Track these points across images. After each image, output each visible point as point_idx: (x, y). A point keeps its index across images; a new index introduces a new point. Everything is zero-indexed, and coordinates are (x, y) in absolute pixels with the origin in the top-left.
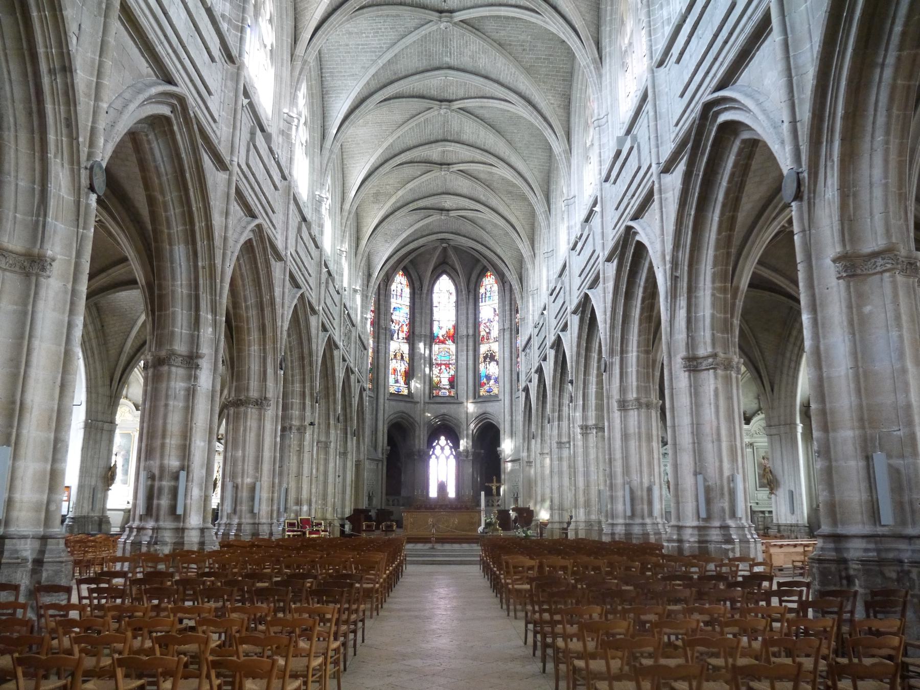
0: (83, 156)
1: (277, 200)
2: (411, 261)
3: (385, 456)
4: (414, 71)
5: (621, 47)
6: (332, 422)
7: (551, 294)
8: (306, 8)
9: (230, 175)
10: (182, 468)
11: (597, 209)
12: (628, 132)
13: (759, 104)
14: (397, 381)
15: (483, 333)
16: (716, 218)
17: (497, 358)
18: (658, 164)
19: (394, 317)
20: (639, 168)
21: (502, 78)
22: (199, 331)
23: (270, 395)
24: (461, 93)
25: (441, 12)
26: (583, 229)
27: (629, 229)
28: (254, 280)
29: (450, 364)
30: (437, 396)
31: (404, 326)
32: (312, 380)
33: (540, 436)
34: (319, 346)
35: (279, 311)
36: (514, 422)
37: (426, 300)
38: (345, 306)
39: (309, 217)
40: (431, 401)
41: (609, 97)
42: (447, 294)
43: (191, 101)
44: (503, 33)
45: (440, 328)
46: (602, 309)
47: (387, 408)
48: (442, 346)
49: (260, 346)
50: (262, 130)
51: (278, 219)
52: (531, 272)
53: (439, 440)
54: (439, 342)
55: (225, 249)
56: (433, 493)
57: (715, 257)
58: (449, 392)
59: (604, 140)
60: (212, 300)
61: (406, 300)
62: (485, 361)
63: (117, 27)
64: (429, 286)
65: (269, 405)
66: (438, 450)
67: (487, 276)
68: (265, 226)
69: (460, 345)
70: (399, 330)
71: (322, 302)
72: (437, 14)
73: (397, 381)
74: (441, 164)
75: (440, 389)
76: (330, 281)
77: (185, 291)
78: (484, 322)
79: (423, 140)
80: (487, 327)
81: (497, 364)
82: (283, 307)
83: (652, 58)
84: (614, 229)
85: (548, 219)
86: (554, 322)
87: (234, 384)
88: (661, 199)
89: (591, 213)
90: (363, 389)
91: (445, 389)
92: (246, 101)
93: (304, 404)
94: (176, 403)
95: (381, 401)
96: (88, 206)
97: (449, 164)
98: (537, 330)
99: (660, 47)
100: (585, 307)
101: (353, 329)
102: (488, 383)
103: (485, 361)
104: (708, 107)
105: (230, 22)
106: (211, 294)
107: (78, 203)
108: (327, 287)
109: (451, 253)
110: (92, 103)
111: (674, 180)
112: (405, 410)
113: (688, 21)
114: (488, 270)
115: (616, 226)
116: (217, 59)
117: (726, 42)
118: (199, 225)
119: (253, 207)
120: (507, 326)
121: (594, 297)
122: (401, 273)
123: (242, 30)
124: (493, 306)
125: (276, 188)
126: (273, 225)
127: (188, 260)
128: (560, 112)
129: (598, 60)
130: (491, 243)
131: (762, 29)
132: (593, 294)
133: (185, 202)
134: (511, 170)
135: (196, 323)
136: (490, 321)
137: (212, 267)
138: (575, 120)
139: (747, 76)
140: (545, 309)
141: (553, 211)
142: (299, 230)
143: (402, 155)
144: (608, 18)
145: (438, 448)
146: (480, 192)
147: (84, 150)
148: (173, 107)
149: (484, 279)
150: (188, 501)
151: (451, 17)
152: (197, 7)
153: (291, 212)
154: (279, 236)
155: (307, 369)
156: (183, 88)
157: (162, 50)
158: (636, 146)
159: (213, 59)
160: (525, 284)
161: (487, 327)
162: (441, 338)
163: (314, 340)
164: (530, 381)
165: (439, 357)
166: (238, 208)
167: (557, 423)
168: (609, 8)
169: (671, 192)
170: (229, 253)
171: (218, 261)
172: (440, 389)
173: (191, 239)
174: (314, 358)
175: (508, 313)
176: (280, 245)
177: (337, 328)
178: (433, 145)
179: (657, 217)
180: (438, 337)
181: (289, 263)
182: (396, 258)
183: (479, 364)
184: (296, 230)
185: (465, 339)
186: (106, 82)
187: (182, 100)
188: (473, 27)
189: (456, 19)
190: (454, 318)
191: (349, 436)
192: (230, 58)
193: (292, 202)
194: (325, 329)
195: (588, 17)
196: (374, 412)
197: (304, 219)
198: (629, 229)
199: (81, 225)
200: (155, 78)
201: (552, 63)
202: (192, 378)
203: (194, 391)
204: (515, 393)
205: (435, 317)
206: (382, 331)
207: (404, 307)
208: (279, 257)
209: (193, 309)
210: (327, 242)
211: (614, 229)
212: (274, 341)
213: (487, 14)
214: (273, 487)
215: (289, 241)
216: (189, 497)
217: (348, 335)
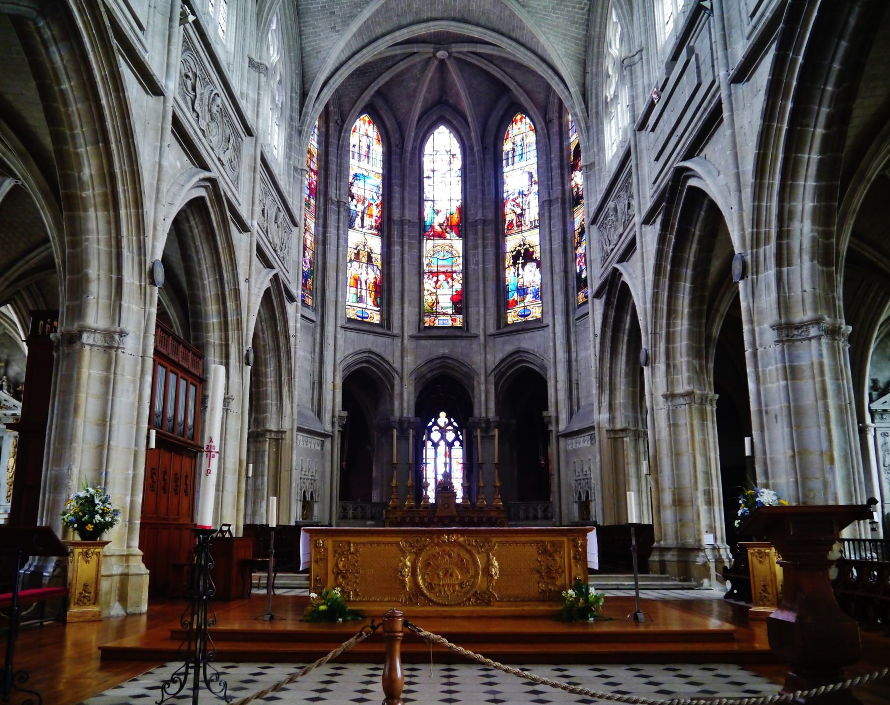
3: (337, 428)
14: (360, 299)
15: (510, 217)
17: (537, 255)
19: (354, 190)
29: (453, 272)
31: (374, 207)
33: (662, 358)
36: (574, 364)
37: (412, 162)
40: (423, 334)
42: (447, 157)
47: (340, 342)
53: (437, 417)
54: (433, 236)
58: (454, 320)
61: (377, 165)
62: (515, 264)
64: (415, 140)
66: (436, 436)
67: (516, 121)
69: (471, 237)
70: (363, 213)
73: (360, 299)
75: (437, 314)
78: (511, 197)
80: (518, 205)
91: (444, 314)
95: (330, 328)
101: (247, 140)
102: (523, 300)
109: (455, 75)
112: (374, 349)
120: (557, 192)
124: (527, 169)
136: (522, 194)
149: (510, 128)
161: (518, 205)
162: (438, 228)
165: (434, 260)
167: (772, 272)
172: (437, 314)
175: (556, 172)
180: (432, 227)
183: (505, 269)
190: (459, 196)
196: (317, 349)
204: (575, 310)
205: (428, 193)
206: (333, 207)
207: (372, 175)
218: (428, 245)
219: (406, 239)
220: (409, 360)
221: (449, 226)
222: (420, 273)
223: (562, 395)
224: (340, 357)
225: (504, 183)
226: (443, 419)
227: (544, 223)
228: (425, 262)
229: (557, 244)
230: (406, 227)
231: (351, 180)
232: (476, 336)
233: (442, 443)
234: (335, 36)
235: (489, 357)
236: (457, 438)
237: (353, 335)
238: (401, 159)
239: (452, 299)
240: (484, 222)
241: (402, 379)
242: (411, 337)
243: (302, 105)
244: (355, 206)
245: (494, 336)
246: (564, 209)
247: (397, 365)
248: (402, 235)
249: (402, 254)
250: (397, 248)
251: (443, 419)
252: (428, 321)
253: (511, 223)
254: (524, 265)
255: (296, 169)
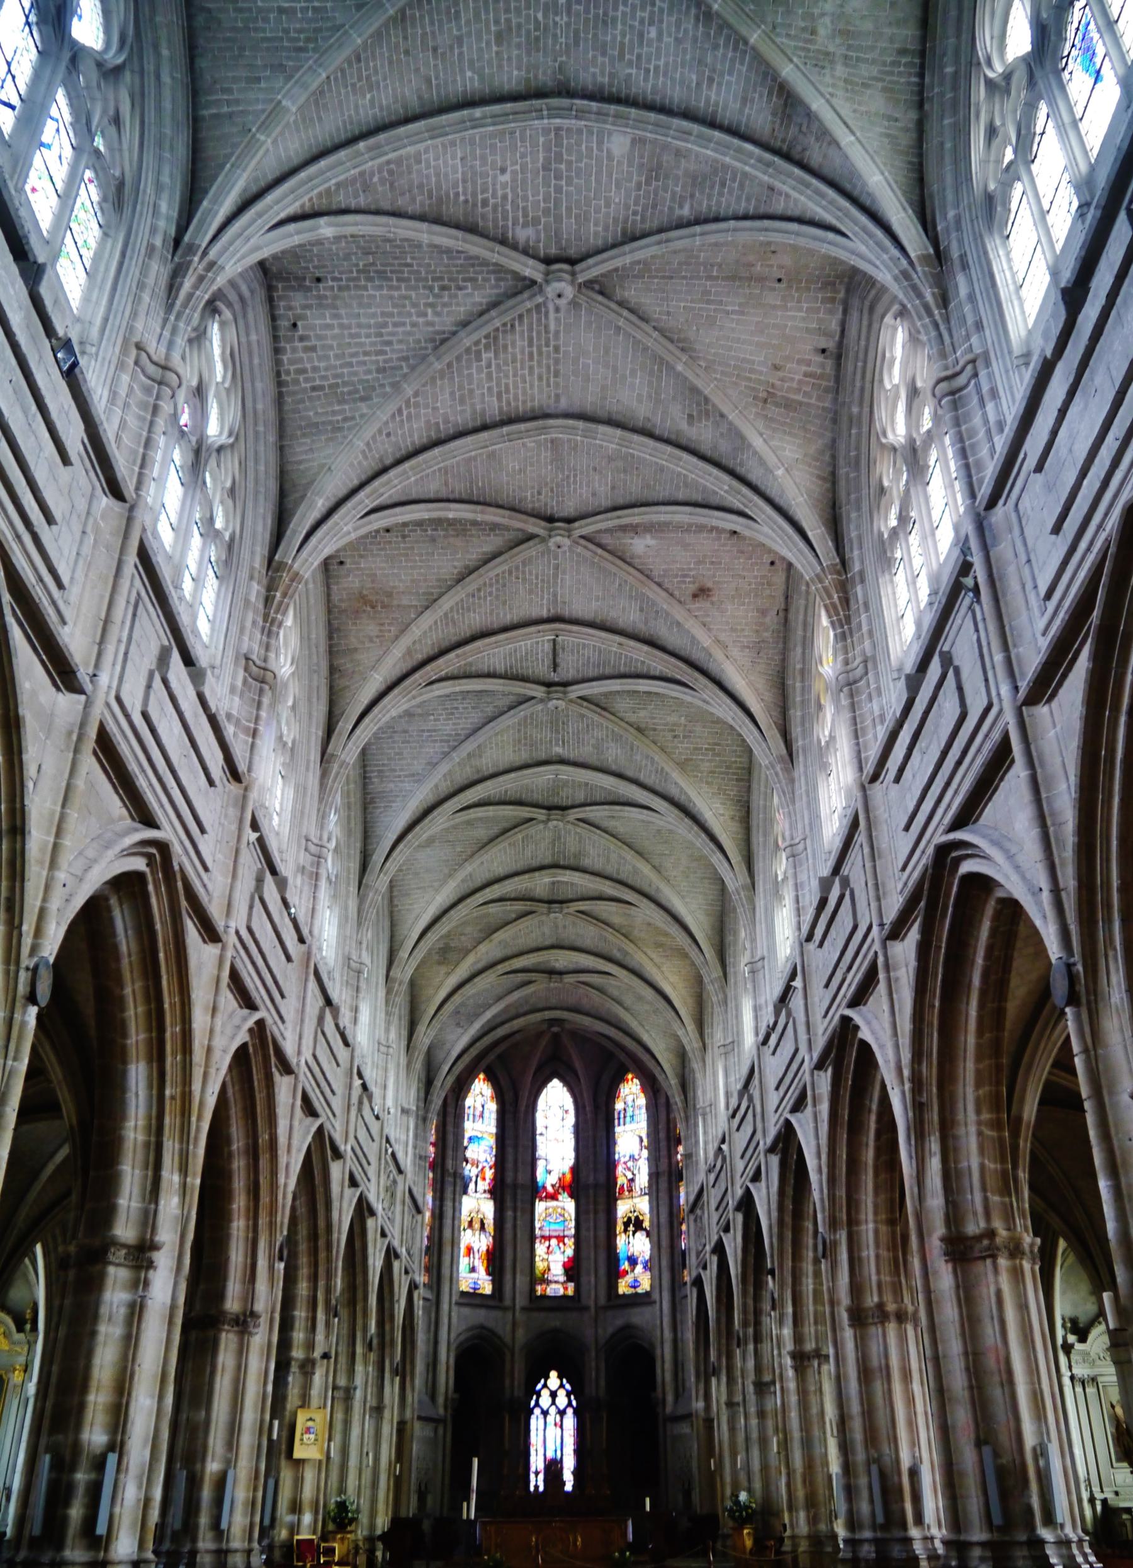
0: (25, 950)
1: (289, 976)
2: (500, 1057)
3: (449, 1411)
4: (507, 766)
5: (819, 741)
6: (359, 1350)
7: (733, 1116)
8: (347, 687)
9: (223, 949)
10: (111, 1447)
11: (798, 983)
12: (836, 870)
13: (1010, 857)
15: (621, 1181)
16: (973, 1012)
17: (646, 1224)
18: (882, 925)
19: (469, 1154)
20: (855, 928)
21: (642, 777)
22: (157, 1203)
23: (260, 1306)
24: (581, 797)
25: (549, 685)
26: (777, 1014)
27: (846, 1021)
28: (245, 1109)
30: (544, 1297)
31: (487, 1169)
32: (329, 1276)
33: (724, 1372)
34: (343, 1215)
35: (283, 1159)
38: (388, 1141)
39: (334, 995)
41: (806, 813)
42: (560, 1113)
43: (176, 849)
44: (642, 713)
45: (549, 1172)
46: (814, 1150)
47: (454, 1320)
48: (554, 1203)
49: (248, 1219)
50: (274, 872)
51: (289, 1008)
52: (698, 1075)
53: (547, 1377)
55: (207, 1066)
56: (537, 1482)
57: (978, 1073)
58: (566, 1289)
59: (803, 877)
60: (181, 1150)
62: (626, 1231)
63: (90, 765)
65: (256, 1326)
66: (545, 1400)
68: (269, 1021)
69: (583, 1201)
71: (351, 1136)
72: (543, 689)
73: (473, 1270)
74: (550, 902)
75: (549, 1282)
76: (365, 1101)
77: (141, 1137)
79: (519, 866)
81: (648, 1235)
82: (289, 1151)
83: (861, 769)
84: (825, 1016)
85: (723, 989)
86: (740, 1165)
87: (202, 1287)
88: (889, 980)
89: (787, 991)
90: (413, 1286)
92: (254, 836)
93: (314, 1320)
94: (111, 1329)
95: (445, 1306)
96: (23, 1024)
97: (561, 902)
98: (712, 1177)
99: (873, 753)
100: (786, 1141)
101: (400, 1179)
103: (626, 1231)
104: (943, 850)
105: (238, 723)
106: (181, 1141)
107: (10, 1022)
108: (360, 1110)
110: (45, 873)
111: (906, 950)
113: (906, 726)
114: (627, 1071)
115: (827, 1012)
116: (217, 781)
117: (959, 763)
118: (172, 1030)
119: (254, 994)
120: (663, 1166)
121: (801, 1126)
122: (482, 1076)
123: (255, 733)
125: (289, 959)
126: (281, 1017)
127: (150, 1087)
128: (735, 827)
129: (787, 758)
130: (634, 1025)
131: (1000, 758)
132: (799, 1121)
133: (153, 996)
134: (662, 912)
135: (153, 1190)
136: (632, 1157)
137: (186, 1097)
138: (757, 839)
139: (991, 813)
140: (723, 1141)
141: (731, 980)
142: (321, 1020)
143: (488, 890)
144: (798, 699)
145: (545, 1394)
146: (614, 943)
147: (27, 942)
148: (150, 857)
150: (117, 1510)
151: (565, 693)
152: (196, 715)
153: (309, 994)
154: (288, 1034)
155: (322, 1255)
156: (168, 832)
157: (144, 783)
158: (848, 893)
159: (211, 783)
160: (690, 1095)
162: (550, 1189)
163: (335, 1205)
164: (705, 1268)
166: (230, 996)
168: (798, 685)
169: (904, 970)
170: (212, 1071)
171: (196, 1087)
172: (549, 1282)
173: (156, 1054)
174: (335, 1236)
175: (663, 1144)
176: (289, 1048)
177: (373, 1179)
178: (537, 874)
179: (886, 1007)
180: (544, 1188)
181: (302, 1077)
182: (474, 1052)
183: (615, 1236)
184: (315, 1021)
185: (591, 1192)
186: (67, 842)
187: (163, 847)
188: (597, 705)
189: (573, 696)
191: (387, 1375)
192: (234, 774)
193: (312, 977)
194: (353, 1183)
195: (768, 696)
197: (328, 1002)
198: (846, 1021)
199: (11, 1054)
200: (129, 821)
201: (719, 755)
202: (139, 1284)
203: (142, 1307)
205: (541, 1151)
208: (287, 1069)
209: (151, 1167)
210: (362, 1036)
211: (825, 1016)
212: (273, 1211)
213: (618, 688)
214: (256, 1477)
215: (304, 1041)
216: (119, 1501)
217: (391, 1190)
218: (540, 1207)
219: (519, 1204)
220: (520, 1333)
221: (563, 1186)
222: (532, 1239)
223: (668, 1377)
224: (453, 1335)
225: (615, 1143)
226: (554, 1380)
227: (653, 1191)
228: (537, 1225)
229: (664, 1218)
230: (519, 1192)
231: (465, 1143)
232: (586, 1308)
233: (553, 1410)
234: (460, 1030)
235: (600, 1331)
236: (570, 1404)
237: (466, 1311)
238: (516, 1112)
239: (564, 1265)
240: (596, 1186)
241: (513, 1355)
242: (523, 1309)
243: (427, 1092)
244: (470, 1171)
245: (606, 1308)
246: (670, 1182)
247: (508, 1339)
248: (515, 1201)
249: (515, 1218)
250: (509, 1213)
251: (554, 1380)
252: (539, 1289)
253: (622, 1186)
254: (634, 1233)
255: (420, 1157)
